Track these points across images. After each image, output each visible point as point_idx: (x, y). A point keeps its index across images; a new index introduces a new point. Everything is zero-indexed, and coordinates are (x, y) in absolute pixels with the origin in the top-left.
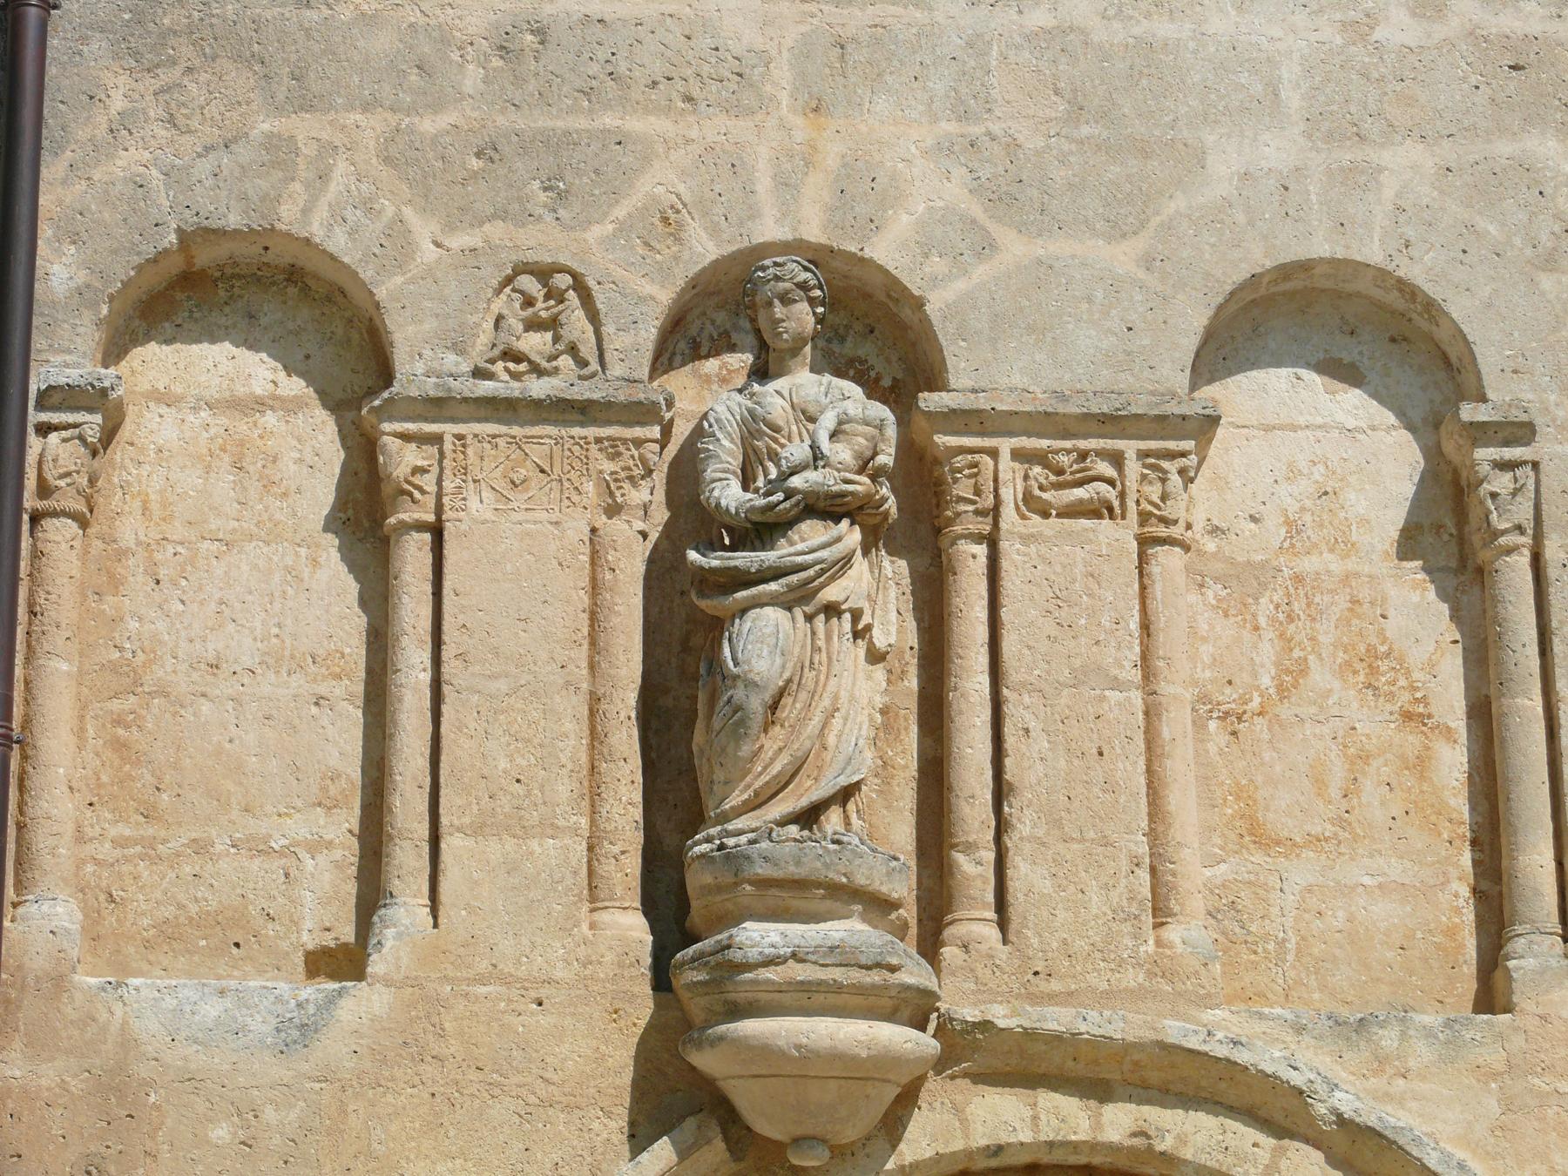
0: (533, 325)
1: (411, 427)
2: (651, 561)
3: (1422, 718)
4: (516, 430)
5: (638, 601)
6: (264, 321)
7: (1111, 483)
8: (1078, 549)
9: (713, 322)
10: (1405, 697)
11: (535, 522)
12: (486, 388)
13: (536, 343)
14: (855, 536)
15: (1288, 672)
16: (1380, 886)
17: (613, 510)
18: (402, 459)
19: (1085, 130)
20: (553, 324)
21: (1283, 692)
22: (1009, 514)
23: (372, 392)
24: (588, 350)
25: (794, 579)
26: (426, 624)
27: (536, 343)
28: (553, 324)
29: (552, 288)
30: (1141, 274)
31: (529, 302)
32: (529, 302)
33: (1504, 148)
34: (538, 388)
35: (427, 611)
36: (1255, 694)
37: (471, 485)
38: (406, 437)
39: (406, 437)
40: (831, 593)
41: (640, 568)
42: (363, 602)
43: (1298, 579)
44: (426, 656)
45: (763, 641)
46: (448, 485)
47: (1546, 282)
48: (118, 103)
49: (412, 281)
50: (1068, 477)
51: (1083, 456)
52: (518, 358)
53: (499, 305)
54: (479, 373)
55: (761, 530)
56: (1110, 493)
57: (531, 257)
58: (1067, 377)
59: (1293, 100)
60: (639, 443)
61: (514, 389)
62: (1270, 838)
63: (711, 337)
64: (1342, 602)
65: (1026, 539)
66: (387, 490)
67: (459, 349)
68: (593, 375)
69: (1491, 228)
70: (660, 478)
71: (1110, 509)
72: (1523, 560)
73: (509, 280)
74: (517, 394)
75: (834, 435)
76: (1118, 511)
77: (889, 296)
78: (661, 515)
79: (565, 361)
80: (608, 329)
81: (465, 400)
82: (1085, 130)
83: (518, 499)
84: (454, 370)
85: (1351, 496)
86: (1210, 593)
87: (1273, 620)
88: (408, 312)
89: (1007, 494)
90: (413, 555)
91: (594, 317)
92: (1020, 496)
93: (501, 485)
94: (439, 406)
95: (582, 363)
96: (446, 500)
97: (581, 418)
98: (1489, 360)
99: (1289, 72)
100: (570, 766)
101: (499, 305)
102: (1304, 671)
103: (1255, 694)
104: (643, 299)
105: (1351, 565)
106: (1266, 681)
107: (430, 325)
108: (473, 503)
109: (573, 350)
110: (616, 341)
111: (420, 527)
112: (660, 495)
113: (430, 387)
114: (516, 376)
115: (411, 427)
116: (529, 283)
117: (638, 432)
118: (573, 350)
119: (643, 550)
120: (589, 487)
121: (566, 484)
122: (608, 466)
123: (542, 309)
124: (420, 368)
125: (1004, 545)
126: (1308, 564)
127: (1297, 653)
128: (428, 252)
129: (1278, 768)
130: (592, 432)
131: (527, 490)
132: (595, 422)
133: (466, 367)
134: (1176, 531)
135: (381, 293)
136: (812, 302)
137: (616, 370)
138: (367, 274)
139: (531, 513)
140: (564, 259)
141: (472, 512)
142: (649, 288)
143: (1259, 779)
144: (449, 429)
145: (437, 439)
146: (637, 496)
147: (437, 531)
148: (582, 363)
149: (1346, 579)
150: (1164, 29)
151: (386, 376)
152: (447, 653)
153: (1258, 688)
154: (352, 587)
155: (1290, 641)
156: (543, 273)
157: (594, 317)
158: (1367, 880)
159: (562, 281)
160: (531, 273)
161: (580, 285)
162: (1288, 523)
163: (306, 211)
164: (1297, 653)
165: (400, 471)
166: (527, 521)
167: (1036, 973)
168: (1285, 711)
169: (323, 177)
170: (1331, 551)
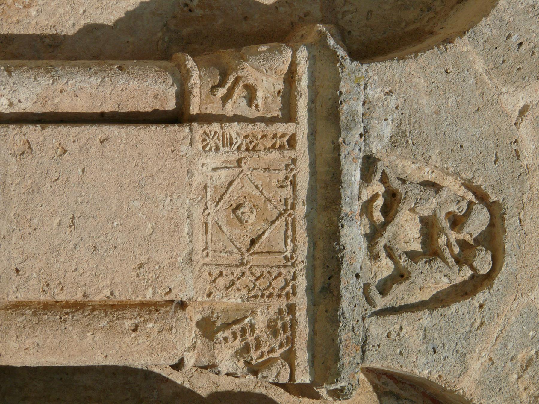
0: (429, 227)
1: (303, 83)
2: (147, 375)
4: (301, 210)
5: (98, 359)
11: (190, 235)
12: (352, 172)
13: (407, 231)
17: (207, 328)
18: (264, 73)
20: (430, 251)
23: (344, 36)
24: (399, 295)
26: (67, 105)
27: (407, 231)
28: (430, 251)
29: (473, 250)
31: (456, 222)
32: (456, 222)
34: (354, 235)
35: (82, 105)
38: (291, 77)
39: (291, 77)
41: (139, 362)
42: (91, 29)
44: (27, 105)
49: (479, 81)
52: (389, 211)
53: (452, 186)
54: (369, 164)
57: (511, 224)
60: (289, 358)
61: (351, 206)
66: (227, 56)
67: (398, 139)
70: (248, 383)
73: (482, 197)
74: (346, 209)
78: (203, 385)
79: (385, 268)
81: (337, 148)
83: (219, 214)
84: (373, 134)
88: (441, 77)
90: (150, 89)
91: (440, 300)
93: (235, 193)
94: (328, 115)
95: (384, 288)
97: (318, 288)
101: (452, 186)
104: (462, 359)
107: (426, 103)
108: (212, 160)
109: (400, 276)
110: (412, 327)
111: (183, 96)
112: (227, 385)
113: (351, 106)
114: (367, 208)
115: (303, 83)
116: (479, 222)
117: (302, 357)
118: (400, 276)
119: (160, 364)
120: (235, 299)
122: (260, 321)
123: (448, 239)
124: (375, 93)
128: (513, 101)
130: (301, 301)
132: (313, 304)
133: (376, 148)
135: (463, 45)
137: (377, 329)
138: (486, 27)
139: (201, 229)
140: (509, 264)
141: (203, 161)
142: (476, 366)
144: (301, 129)
145: (289, 115)
146: (226, 358)
147: (178, 117)
148: (384, 288)
151: (364, 53)
152: (32, 132)
154: (109, 16)
156: (491, 239)
157: (440, 300)
159: (483, 262)
160: (491, 225)
161: (478, 283)
165: (249, 71)
166: (192, 225)
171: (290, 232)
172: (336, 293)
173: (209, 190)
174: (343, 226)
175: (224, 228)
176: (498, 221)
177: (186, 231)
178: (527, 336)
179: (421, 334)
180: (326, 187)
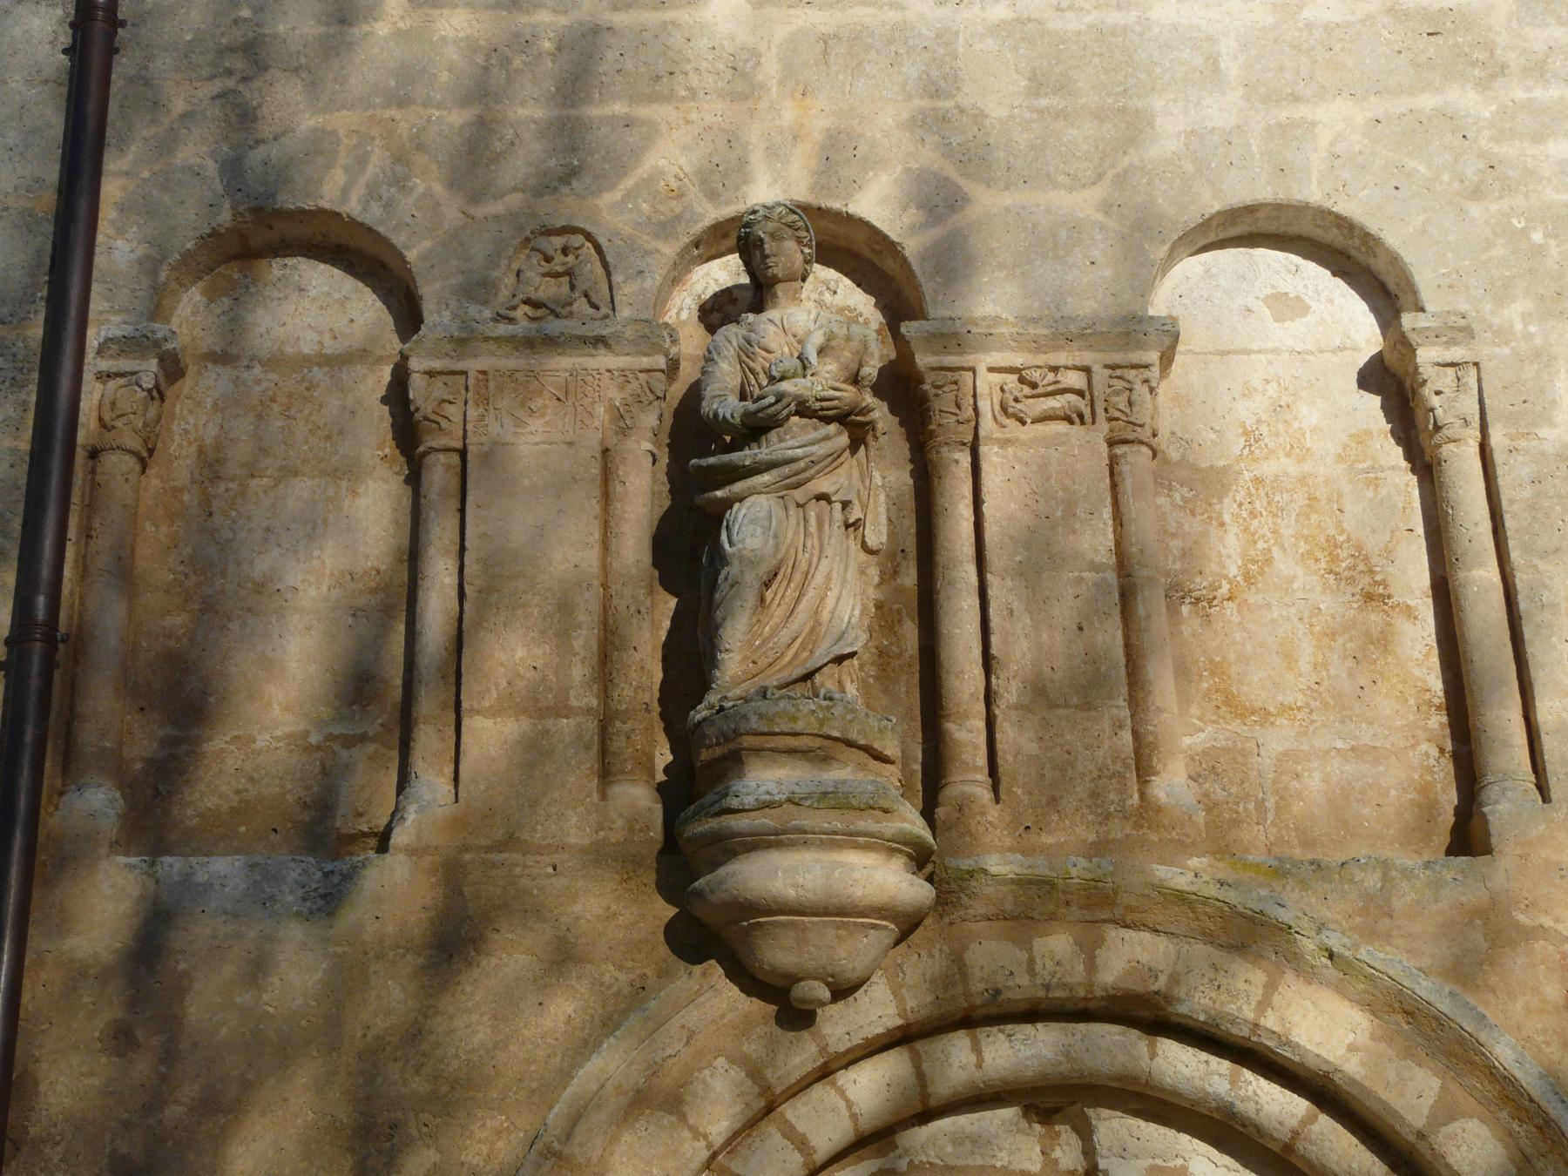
3: (1385, 598)
6: (313, 293)
7: (1080, 393)
8: (1052, 451)
10: (1366, 580)
14: (844, 439)
15: (1254, 561)
16: (1353, 749)
19: (1044, 102)
21: (1247, 576)
22: (987, 425)
25: (786, 470)
30: (1100, 217)
33: (1427, 102)
36: (1224, 582)
37: (492, 411)
40: (823, 485)
43: (1258, 481)
45: (754, 523)
46: (473, 413)
47: (1475, 209)
48: (179, 106)
50: (1040, 390)
51: (1055, 369)
55: (756, 428)
56: (1082, 405)
58: (1036, 304)
59: (1232, 69)
62: (1246, 708)
64: (1301, 499)
65: (1005, 443)
68: (606, 317)
69: (1422, 169)
71: (1081, 416)
72: (1472, 449)
75: (821, 352)
76: (1088, 416)
77: (873, 250)
79: (581, 305)
80: (618, 278)
82: (1044, 102)
85: (1304, 409)
86: (1177, 496)
87: (1236, 517)
89: (984, 405)
92: (997, 408)
96: (469, 427)
98: (1426, 279)
99: (1227, 46)
100: (583, 653)
102: (1269, 561)
103: (1224, 582)
105: (1307, 467)
106: (1233, 570)
121: (579, 409)
125: (983, 449)
126: (1267, 469)
127: (1261, 545)
129: (1249, 647)
131: (543, 416)
134: (1144, 434)
136: (799, 241)
143: (1232, 657)
145: (464, 373)
149: (1303, 480)
150: (1114, 18)
153: (1226, 577)
155: (1253, 534)
158: (1340, 744)
162: (1246, 433)
163: (345, 191)
164: (1261, 545)
167: (1027, 828)
168: (1253, 598)
169: (362, 161)
170: (1288, 455)
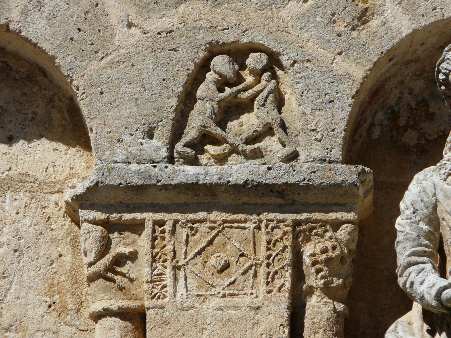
9: (411, 92)
11: (236, 308)
57: (228, 37)
63: (409, 105)
81: (166, 187)
131: (229, 276)
139: (233, 299)
142: (343, 65)
156: (238, 54)
166: (229, 308)
171: (235, 225)
172: (284, 187)
173: (200, 293)
174: (229, 182)
175: (232, 279)
176: (225, 48)
177: (233, 312)
178: (320, 22)
179: (318, 113)
180: (197, 195)
